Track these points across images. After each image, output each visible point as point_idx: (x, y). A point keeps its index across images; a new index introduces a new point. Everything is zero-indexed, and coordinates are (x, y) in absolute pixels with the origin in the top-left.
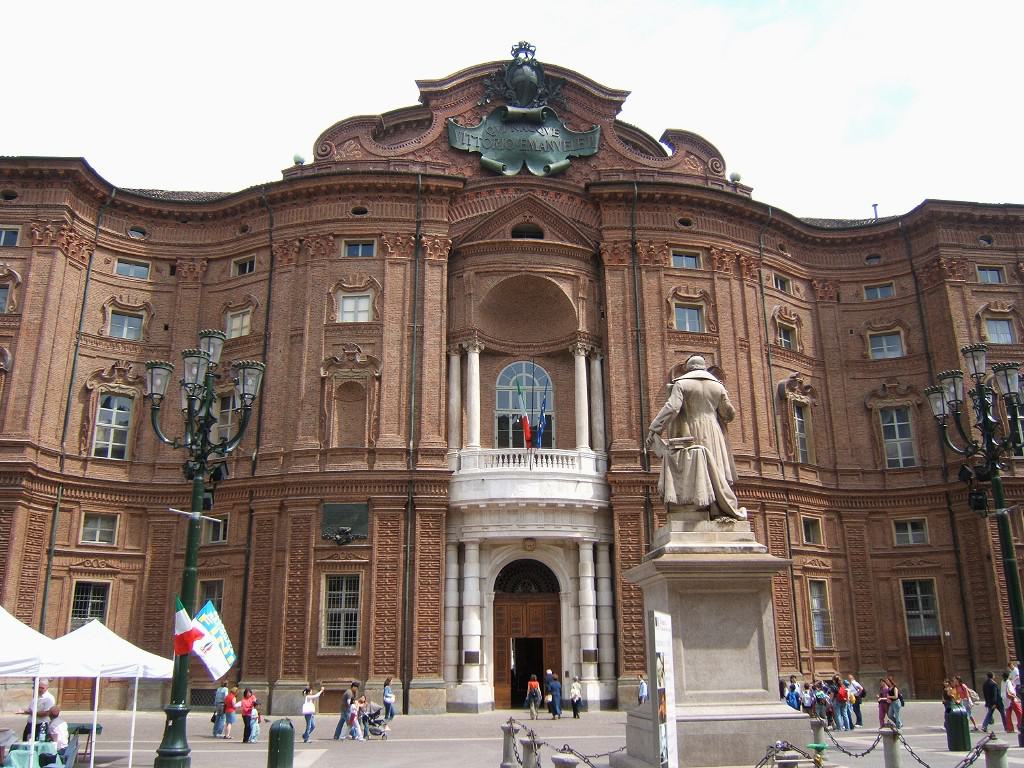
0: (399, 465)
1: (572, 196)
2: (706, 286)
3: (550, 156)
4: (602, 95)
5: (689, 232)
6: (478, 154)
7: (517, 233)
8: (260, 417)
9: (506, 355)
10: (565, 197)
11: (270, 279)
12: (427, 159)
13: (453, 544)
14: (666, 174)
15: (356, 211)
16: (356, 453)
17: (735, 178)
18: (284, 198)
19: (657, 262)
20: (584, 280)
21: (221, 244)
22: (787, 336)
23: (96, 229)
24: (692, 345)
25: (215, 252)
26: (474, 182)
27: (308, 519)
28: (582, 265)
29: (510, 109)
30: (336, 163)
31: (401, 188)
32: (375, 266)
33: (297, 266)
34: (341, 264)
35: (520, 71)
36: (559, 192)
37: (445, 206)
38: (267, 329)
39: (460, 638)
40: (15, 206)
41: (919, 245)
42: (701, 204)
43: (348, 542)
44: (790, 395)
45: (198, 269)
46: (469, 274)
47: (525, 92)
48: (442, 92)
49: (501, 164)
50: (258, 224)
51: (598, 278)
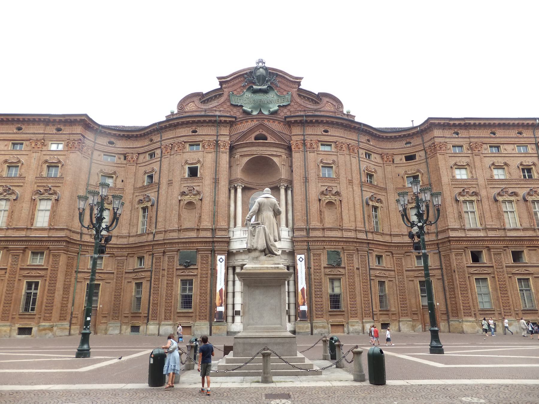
0: (209, 234)
1: (279, 122)
2: (334, 158)
3: (270, 106)
4: (292, 79)
5: (327, 135)
6: (242, 106)
7: (256, 138)
8: (157, 216)
9: (254, 189)
10: (277, 122)
11: (161, 160)
12: (221, 109)
13: (231, 267)
14: (318, 111)
15: (193, 132)
16: (192, 230)
17: (348, 112)
18: (166, 127)
19: (314, 148)
20: (284, 156)
21: (143, 147)
22: (371, 178)
23: (94, 142)
24: (328, 183)
25: (141, 150)
26: (240, 118)
27: (173, 257)
28: (283, 151)
29: (255, 87)
30: (185, 112)
31: (210, 121)
32: (200, 154)
33: (170, 155)
34: (187, 154)
35: (258, 71)
36: (274, 121)
37: (228, 128)
38: (159, 181)
39: (234, 305)
40: (62, 134)
41: (427, 137)
42: (332, 123)
43: (189, 266)
44: (371, 203)
45: (134, 157)
46: (237, 156)
47: (262, 79)
48: (227, 81)
49: (250, 110)
50: (156, 138)
51: (290, 155)
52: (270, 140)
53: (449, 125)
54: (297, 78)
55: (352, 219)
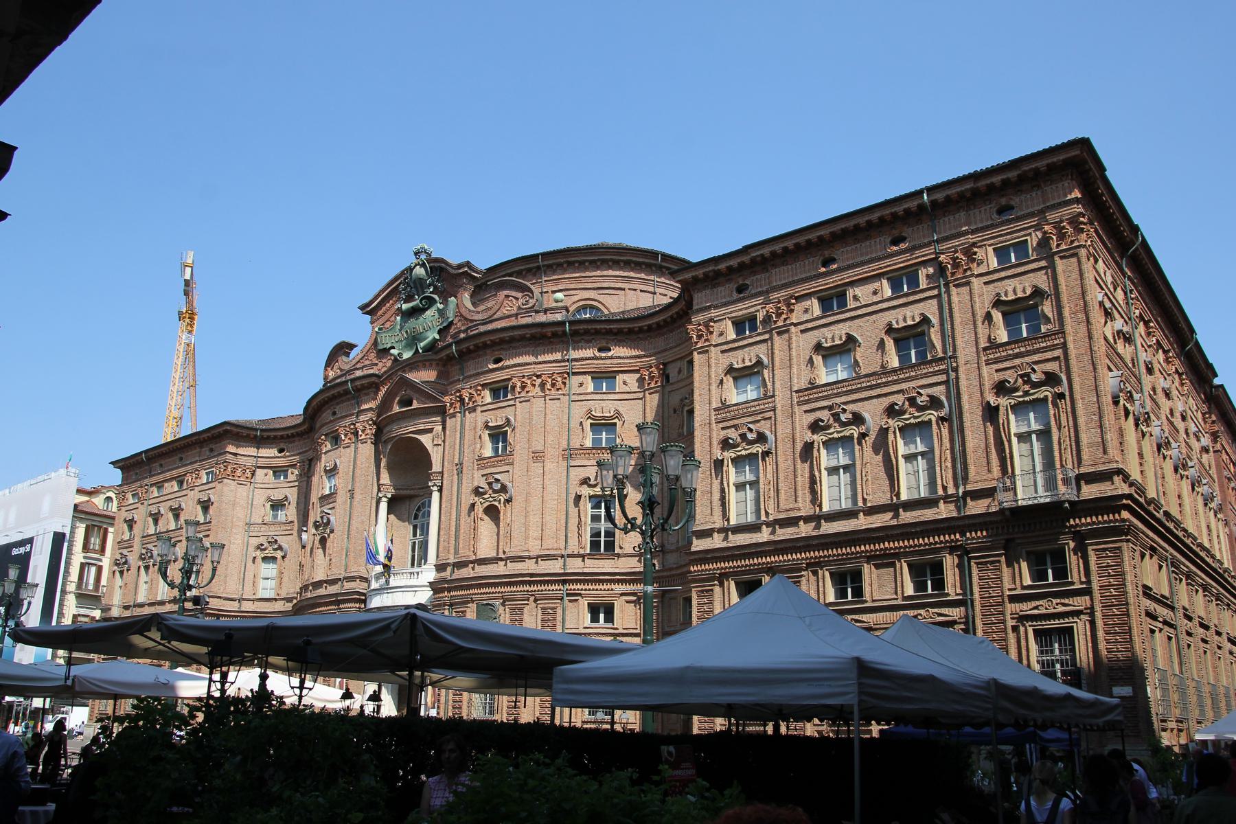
12: (367, 362)
52: (415, 405)
53: (718, 274)
54: (460, 266)
55: (534, 532)
